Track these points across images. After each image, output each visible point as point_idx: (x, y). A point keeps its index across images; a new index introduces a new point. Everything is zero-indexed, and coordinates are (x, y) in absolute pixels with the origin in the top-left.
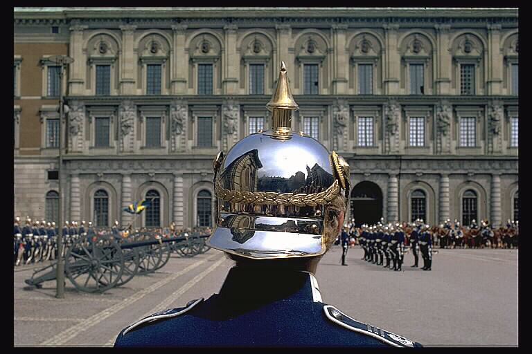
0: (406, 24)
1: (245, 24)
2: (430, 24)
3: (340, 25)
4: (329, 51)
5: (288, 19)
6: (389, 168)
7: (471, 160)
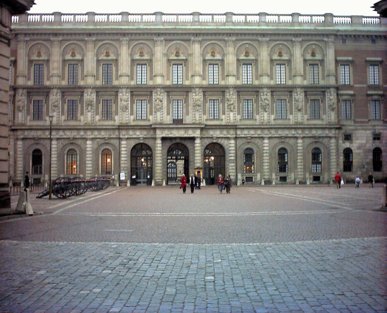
0: (239, 37)
1: (134, 37)
2: (254, 37)
3: (197, 39)
4: (191, 55)
5: (162, 34)
6: (229, 134)
7: (277, 128)
